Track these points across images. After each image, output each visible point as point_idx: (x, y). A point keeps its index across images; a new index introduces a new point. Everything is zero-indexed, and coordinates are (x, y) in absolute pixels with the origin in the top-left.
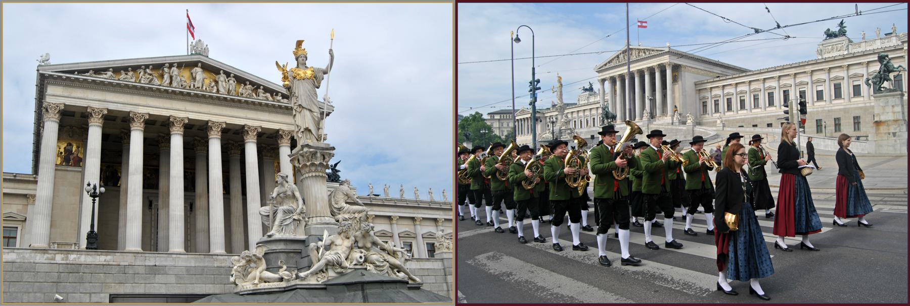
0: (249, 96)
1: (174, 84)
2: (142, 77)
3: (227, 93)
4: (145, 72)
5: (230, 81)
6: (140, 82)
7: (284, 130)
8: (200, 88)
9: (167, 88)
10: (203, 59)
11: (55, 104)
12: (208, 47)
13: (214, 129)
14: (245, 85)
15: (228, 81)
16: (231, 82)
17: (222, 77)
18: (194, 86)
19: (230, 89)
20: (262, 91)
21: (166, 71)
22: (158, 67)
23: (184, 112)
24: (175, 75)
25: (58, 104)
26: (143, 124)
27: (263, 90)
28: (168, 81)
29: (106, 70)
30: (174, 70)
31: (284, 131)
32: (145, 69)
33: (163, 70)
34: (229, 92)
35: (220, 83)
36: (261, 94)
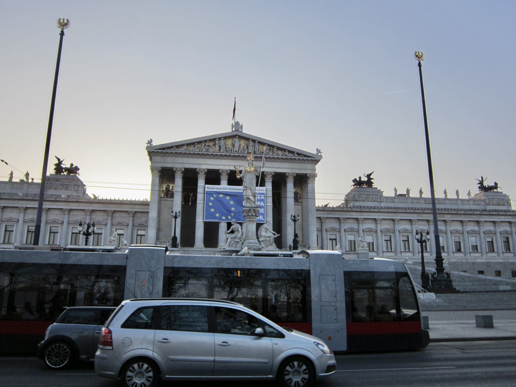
0: (266, 154)
1: (222, 150)
9: (217, 153)
10: (239, 134)
15: (254, 145)
16: (256, 146)
18: (234, 149)
19: (255, 150)
20: (275, 149)
22: (213, 140)
24: (223, 145)
26: (204, 175)
27: (276, 148)
29: (183, 145)
31: (289, 173)
33: (215, 142)
35: (249, 147)
36: (275, 152)
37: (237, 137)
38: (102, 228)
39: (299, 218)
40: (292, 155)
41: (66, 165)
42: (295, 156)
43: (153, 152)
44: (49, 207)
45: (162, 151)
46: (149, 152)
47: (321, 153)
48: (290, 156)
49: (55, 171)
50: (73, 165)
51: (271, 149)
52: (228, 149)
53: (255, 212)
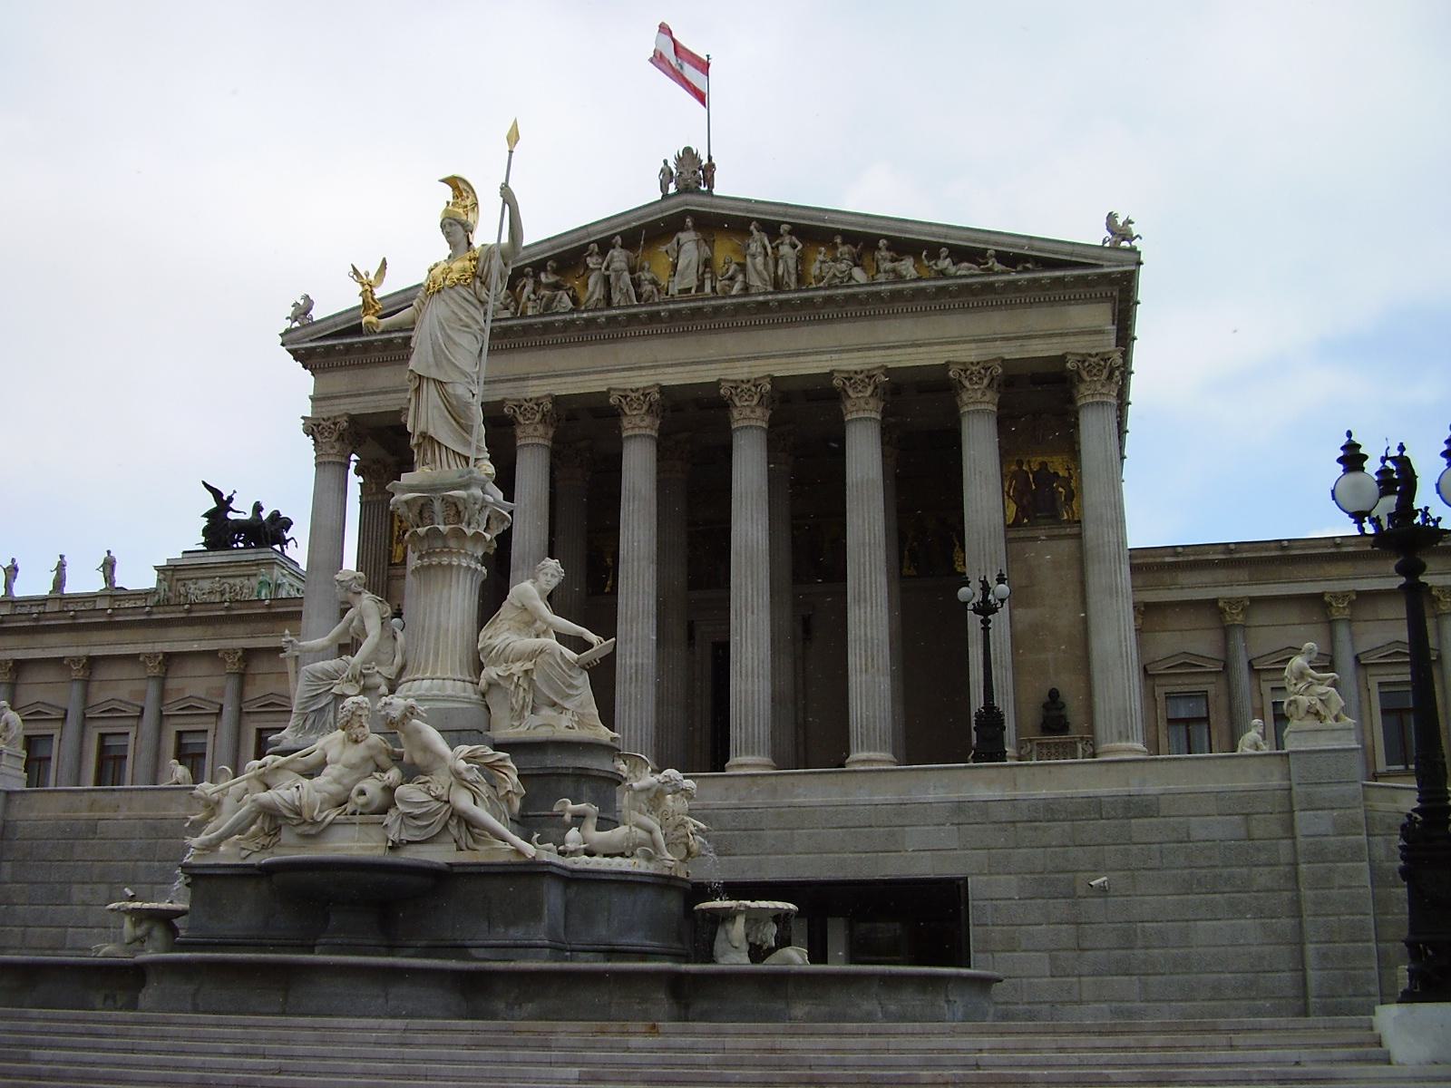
0: (837, 281)
1: (616, 297)
2: (529, 299)
3: (770, 289)
4: (538, 283)
5: (780, 248)
6: (523, 315)
7: (964, 363)
8: (693, 291)
10: (693, 202)
11: (329, 419)
12: (713, 161)
13: (738, 404)
14: (835, 247)
16: (785, 250)
17: (758, 242)
19: (780, 273)
21: (591, 266)
23: (652, 372)
25: (335, 417)
26: (541, 428)
27: (888, 249)
28: (599, 293)
30: (612, 254)
31: (965, 367)
32: (536, 276)
34: (778, 285)
35: (748, 259)
37: (689, 221)
38: (206, 731)
39: (1003, 589)
40: (976, 270)
41: (241, 510)
42: (990, 269)
43: (315, 348)
44: (20, 655)
45: (348, 341)
46: (297, 355)
47: (1131, 239)
48: (959, 273)
49: (203, 539)
50: (262, 509)
51: (860, 256)
52: (647, 288)
53: (458, 513)
